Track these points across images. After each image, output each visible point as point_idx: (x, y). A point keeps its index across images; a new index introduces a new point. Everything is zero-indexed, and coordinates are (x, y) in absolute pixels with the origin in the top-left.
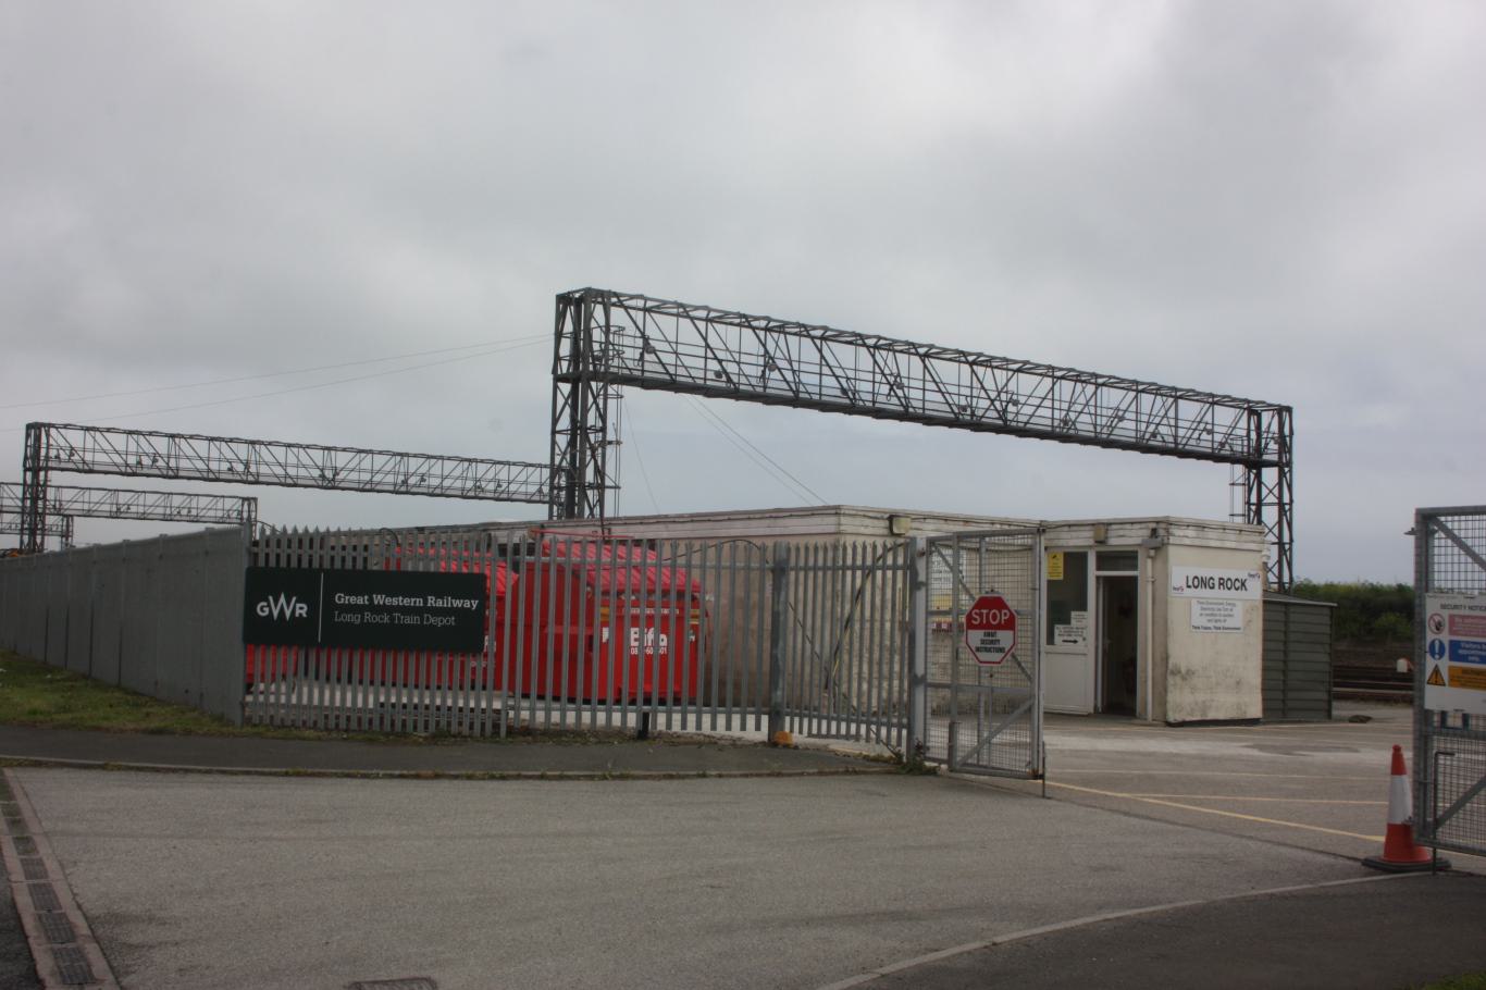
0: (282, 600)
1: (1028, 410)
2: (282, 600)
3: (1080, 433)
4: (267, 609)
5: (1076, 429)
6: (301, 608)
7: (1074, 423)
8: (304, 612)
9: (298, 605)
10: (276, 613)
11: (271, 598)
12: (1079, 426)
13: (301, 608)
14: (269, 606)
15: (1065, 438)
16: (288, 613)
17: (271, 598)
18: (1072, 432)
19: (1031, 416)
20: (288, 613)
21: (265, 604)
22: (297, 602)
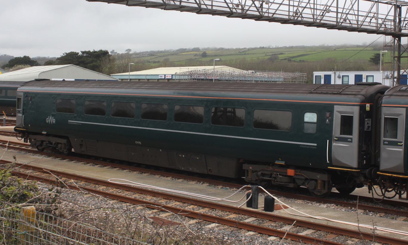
0: (51, 118)
1: (275, 6)
2: (51, 118)
3: (305, 19)
4: (48, 120)
5: (302, 17)
6: (54, 120)
7: (301, 14)
8: (54, 122)
9: (54, 119)
10: (50, 121)
11: (49, 117)
12: (304, 15)
13: (54, 120)
14: (48, 119)
15: (296, 23)
16: (52, 122)
17: (49, 117)
18: (300, 19)
19: (276, 10)
20: (52, 122)
21: (47, 119)
22: (53, 118)
